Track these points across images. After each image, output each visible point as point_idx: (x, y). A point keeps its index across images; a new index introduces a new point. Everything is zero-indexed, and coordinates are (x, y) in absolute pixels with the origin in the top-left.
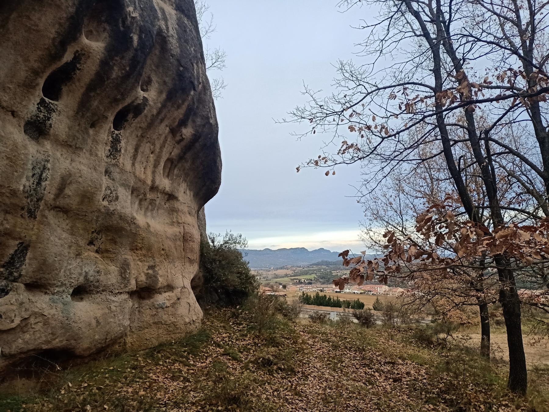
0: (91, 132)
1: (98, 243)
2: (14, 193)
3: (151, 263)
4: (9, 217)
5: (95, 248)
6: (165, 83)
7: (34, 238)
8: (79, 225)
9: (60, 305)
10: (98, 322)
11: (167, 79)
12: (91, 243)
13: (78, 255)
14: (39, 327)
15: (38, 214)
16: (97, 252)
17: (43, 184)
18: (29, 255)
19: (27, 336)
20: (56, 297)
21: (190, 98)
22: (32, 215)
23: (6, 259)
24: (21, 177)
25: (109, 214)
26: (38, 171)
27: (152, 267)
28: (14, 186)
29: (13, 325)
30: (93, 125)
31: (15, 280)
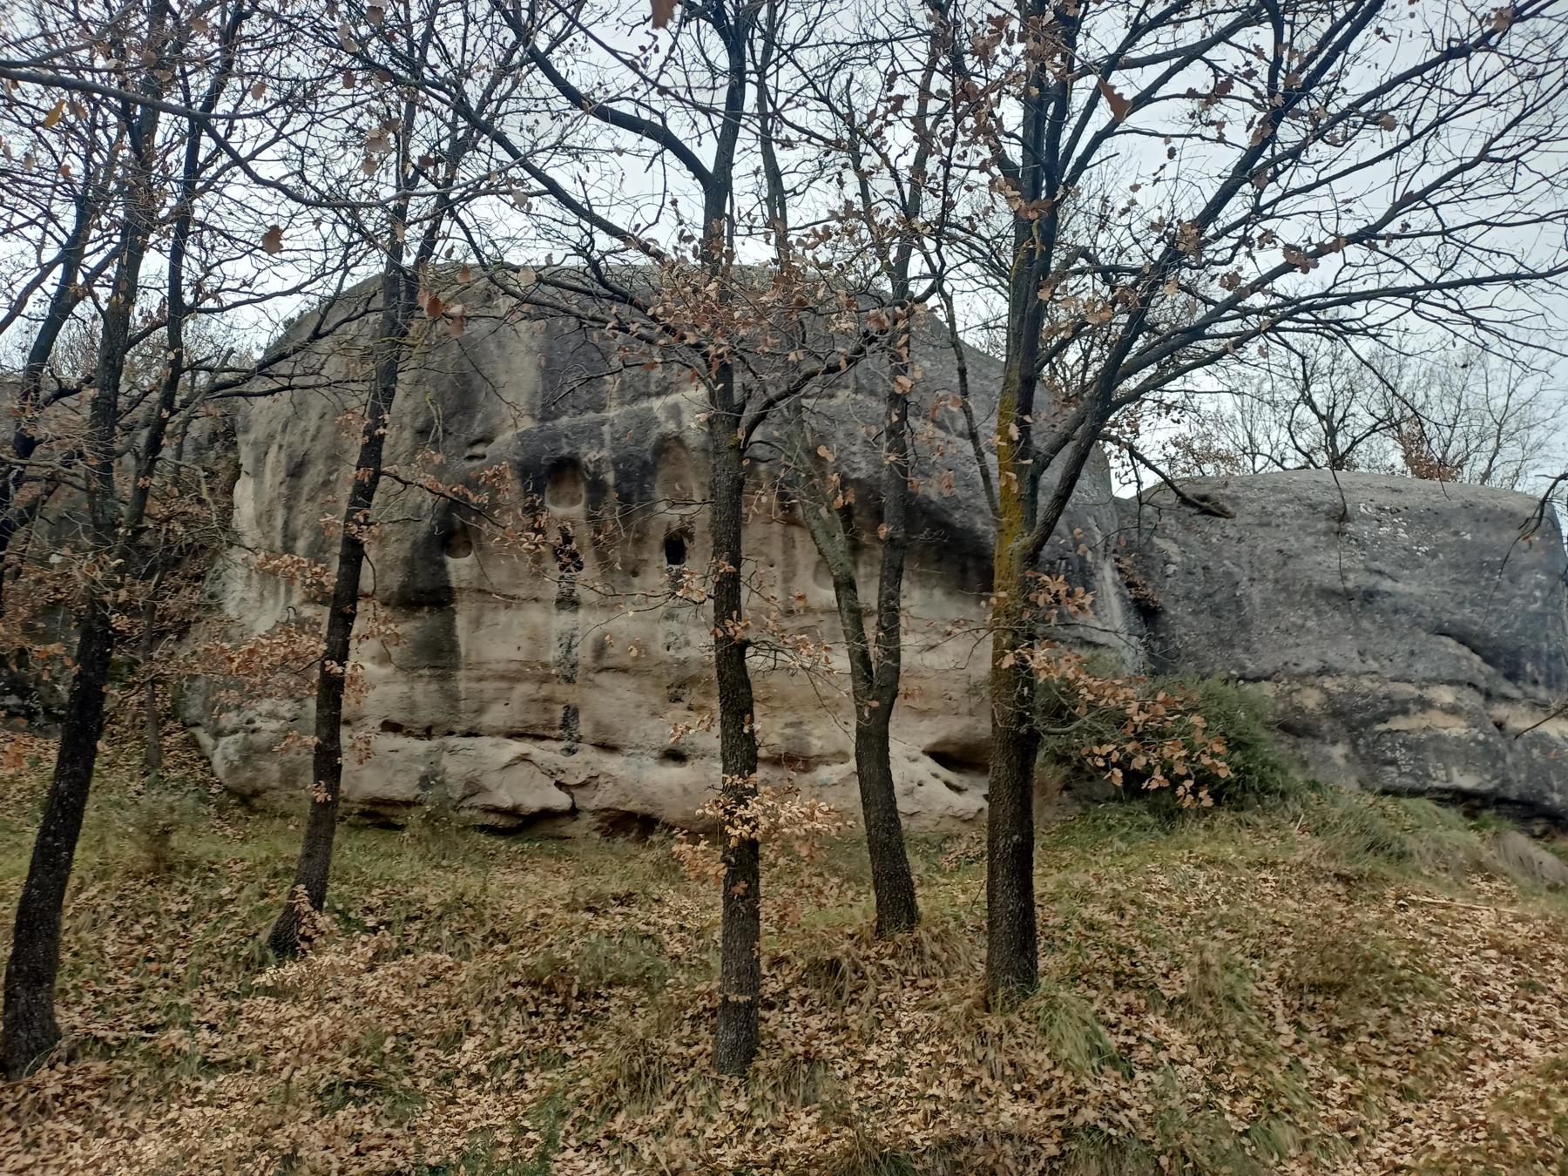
0: (636, 581)
1: (687, 700)
2: (545, 665)
3: (793, 718)
4: (545, 686)
5: (686, 705)
6: (703, 484)
7: (578, 701)
8: (647, 682)
9: (634, 767)
10: (685, 790)
11: (703, 479)
12: (678, 700)
13: (654, 714)
14: (609, 786)
15: (578, 679)
16: (690, 709)
17: (574, 651)
18: (582, 717)
19: (600, 795)
20: (632, 759)
21: (763, 476)
22: (569, 680)
23: (559, 722)
24: (548, 650)
25: (683, 663)
26: (565, 641)
27: (797, 725)
28: (543, 659)
29: (578, 781)
30: (635, 574)
31: (578, 741)
